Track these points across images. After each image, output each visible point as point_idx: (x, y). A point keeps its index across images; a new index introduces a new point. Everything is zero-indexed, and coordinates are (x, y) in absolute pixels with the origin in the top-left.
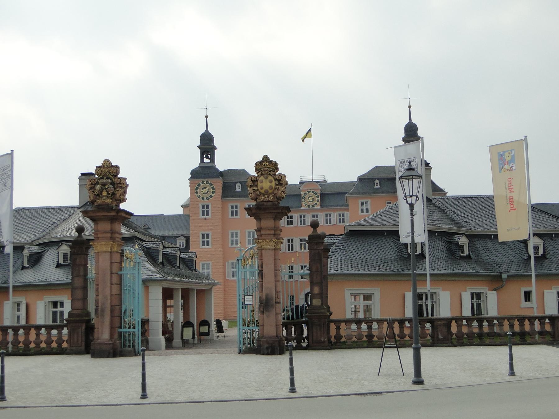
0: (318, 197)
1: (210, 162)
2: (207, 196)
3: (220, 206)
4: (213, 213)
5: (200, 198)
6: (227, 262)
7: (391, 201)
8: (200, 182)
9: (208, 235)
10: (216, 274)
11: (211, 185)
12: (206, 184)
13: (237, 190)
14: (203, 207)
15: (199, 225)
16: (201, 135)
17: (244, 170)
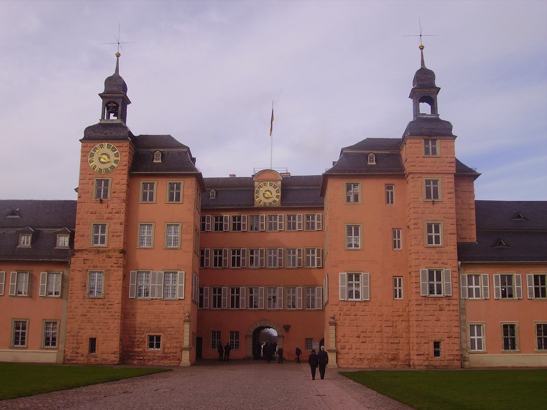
0: (277, 192)
1: (118, 118)
2: (108, 166)
3: (125, 182)
4: (114, 192)
5: (96, 169)
6: (131, 272)
7: (393, 185)
8: (98, 145)
9: (104, 226)
10: (111, 288)
11: (113, 150)
12: (106, 148)
13: (155, 161)
14: (99, 182)
15: (90, 211)
16: (107, 79)
17: (169, 136)
